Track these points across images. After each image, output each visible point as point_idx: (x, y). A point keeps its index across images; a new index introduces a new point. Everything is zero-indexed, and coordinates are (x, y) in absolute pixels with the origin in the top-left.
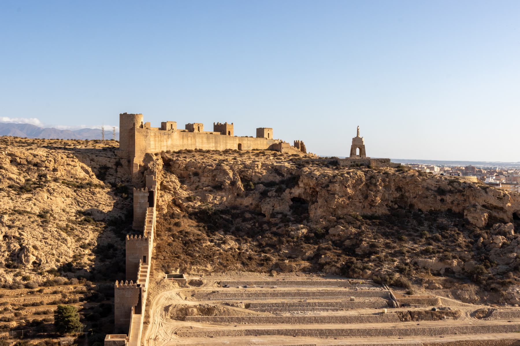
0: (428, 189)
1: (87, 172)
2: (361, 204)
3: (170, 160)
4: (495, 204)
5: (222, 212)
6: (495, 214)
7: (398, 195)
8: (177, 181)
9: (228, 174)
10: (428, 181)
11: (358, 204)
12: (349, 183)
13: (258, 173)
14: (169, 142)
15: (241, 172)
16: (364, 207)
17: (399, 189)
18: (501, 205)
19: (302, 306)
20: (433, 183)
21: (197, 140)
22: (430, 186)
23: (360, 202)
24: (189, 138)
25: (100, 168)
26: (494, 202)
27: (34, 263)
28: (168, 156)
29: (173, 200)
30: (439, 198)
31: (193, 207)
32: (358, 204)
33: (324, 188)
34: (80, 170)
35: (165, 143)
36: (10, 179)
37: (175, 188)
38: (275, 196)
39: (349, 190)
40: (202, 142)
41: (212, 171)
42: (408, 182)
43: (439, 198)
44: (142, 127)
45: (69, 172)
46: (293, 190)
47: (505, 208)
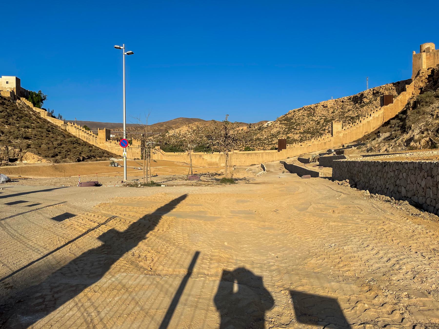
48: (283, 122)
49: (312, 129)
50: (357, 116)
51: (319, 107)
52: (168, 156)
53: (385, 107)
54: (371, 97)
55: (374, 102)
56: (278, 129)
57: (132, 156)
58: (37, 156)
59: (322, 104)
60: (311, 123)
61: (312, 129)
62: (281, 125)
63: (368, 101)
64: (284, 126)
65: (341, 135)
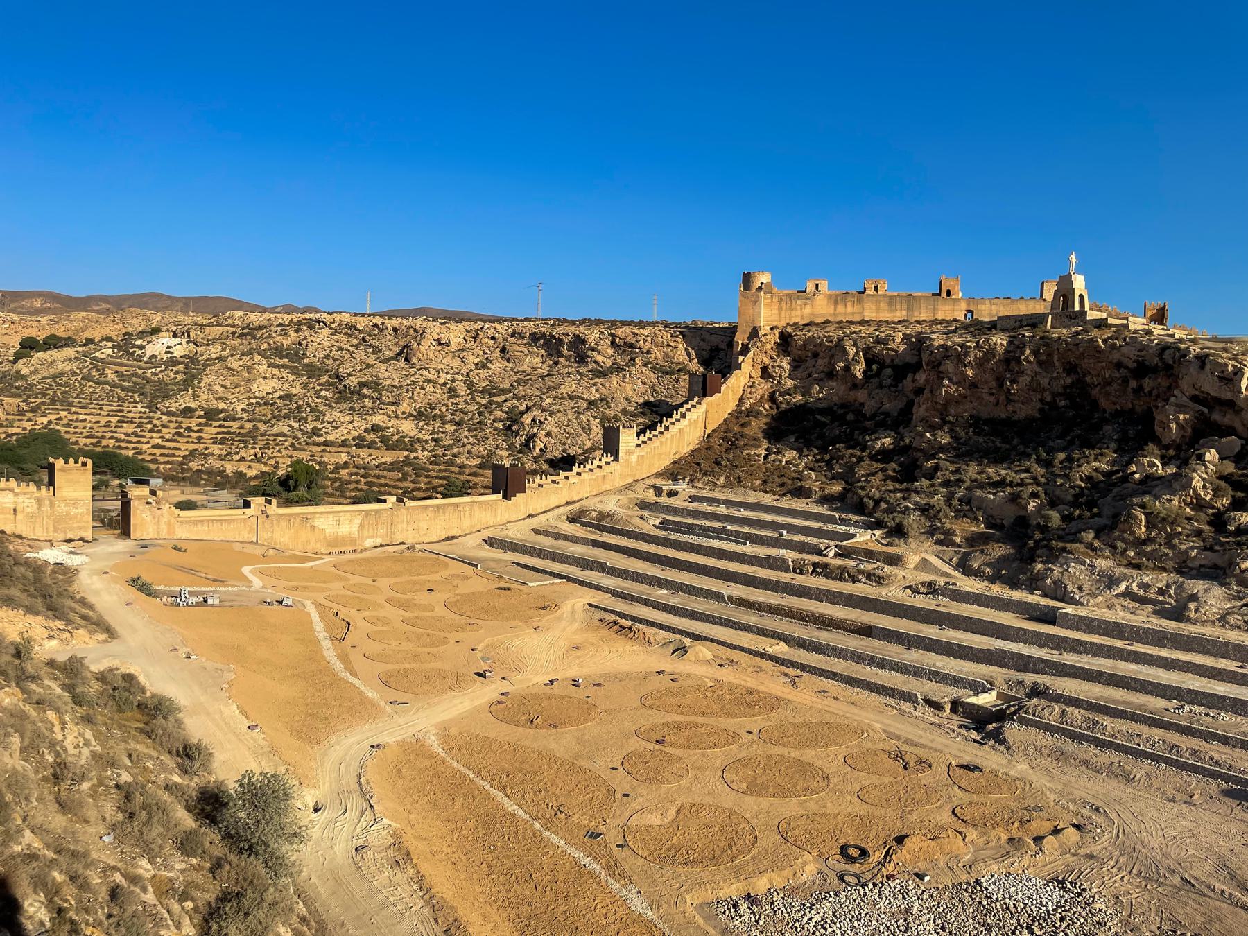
0: (1119, 365)
1: (689, 355)
2: (992, 399)
3: (790, 335)
4: (1213, 393)
5: (822, 411)
6: (1216, 416)
7: (1069, 381)
8: (787, 366)
9: (847, 353)
10: (1125, 350)
11: (986, 397)
12: (970, 358)
13: (893, 350)
14: (808, 310)
15: (867, 351)
16: (997, 404)
17: (1070, 369)
18: (1228, 395)
19: (690, 529)
20: (1131, 352)
21: (866, 305)
22: (1125, 360)
23: (992, 394)
24: (849, 304)
25: (711, 350)
26: (1210, 386)
27: (541, 450)
28: (789, 330)
29: (773, 393)
30: (1133, 384)
31: (788, 403)
32: (986, 397)
33: (934, 367)
34: (681, 352)
35: (799, 312)
36: (596, 362)
37: (780, 376)
38: (891, 385)
39: (970, 372)
40: (878, 310)
41: (830, 348)
42: (1082, 354)
43: (1133, 384)
44: (760, 289)
45: (666, 354)
46: (917, 377)
47: (1238, 402)
48: (278, 361)
49: (444, 409)
50: (602, 400)
51: (425, 344)
52: (196, 523)
53: (707, 400)
54: (610, 351)
55: (633, 370)
56: (272, 383)
57: (56, 530)
58: (40, 619)
59: (436, 337)
60: (430, 388)
61: (444, 409)
62: (275, 371)
63: (609, 363)
64: (291, 377)
65: (634, 458)
